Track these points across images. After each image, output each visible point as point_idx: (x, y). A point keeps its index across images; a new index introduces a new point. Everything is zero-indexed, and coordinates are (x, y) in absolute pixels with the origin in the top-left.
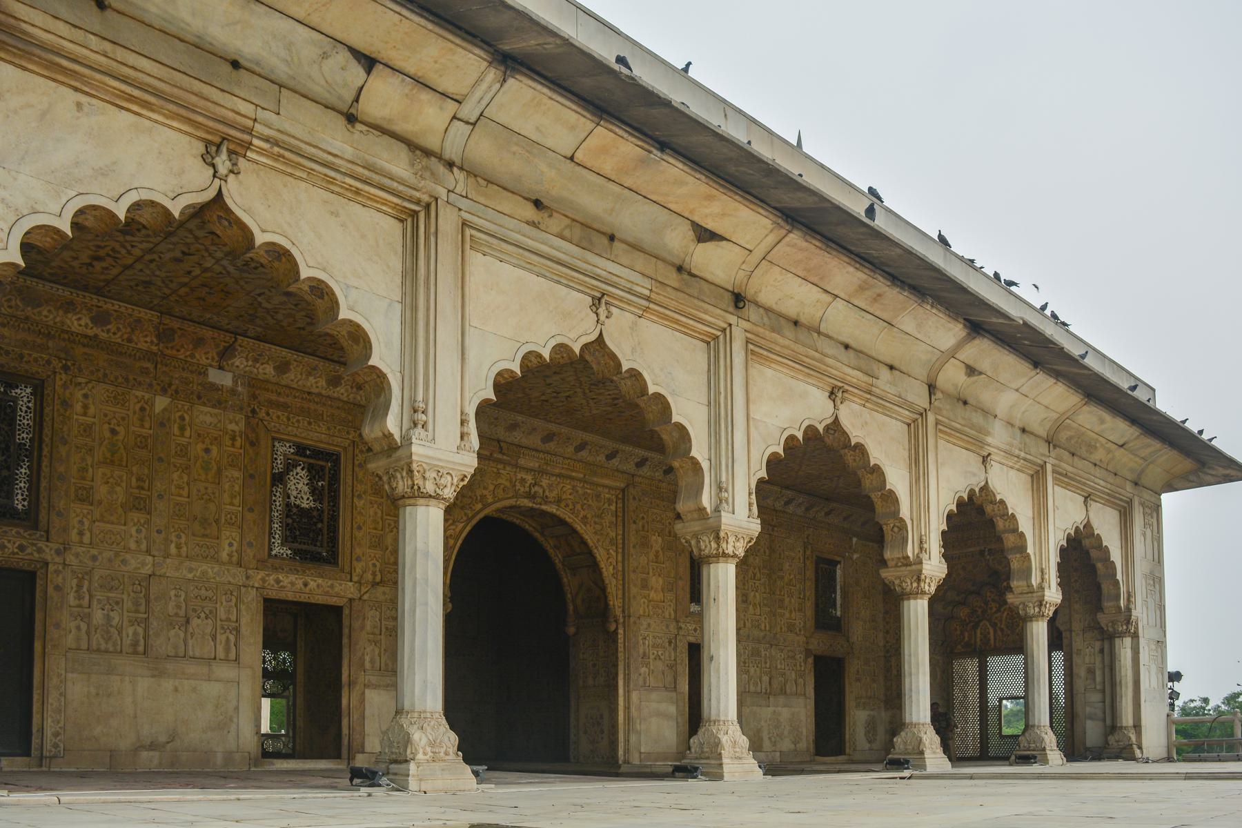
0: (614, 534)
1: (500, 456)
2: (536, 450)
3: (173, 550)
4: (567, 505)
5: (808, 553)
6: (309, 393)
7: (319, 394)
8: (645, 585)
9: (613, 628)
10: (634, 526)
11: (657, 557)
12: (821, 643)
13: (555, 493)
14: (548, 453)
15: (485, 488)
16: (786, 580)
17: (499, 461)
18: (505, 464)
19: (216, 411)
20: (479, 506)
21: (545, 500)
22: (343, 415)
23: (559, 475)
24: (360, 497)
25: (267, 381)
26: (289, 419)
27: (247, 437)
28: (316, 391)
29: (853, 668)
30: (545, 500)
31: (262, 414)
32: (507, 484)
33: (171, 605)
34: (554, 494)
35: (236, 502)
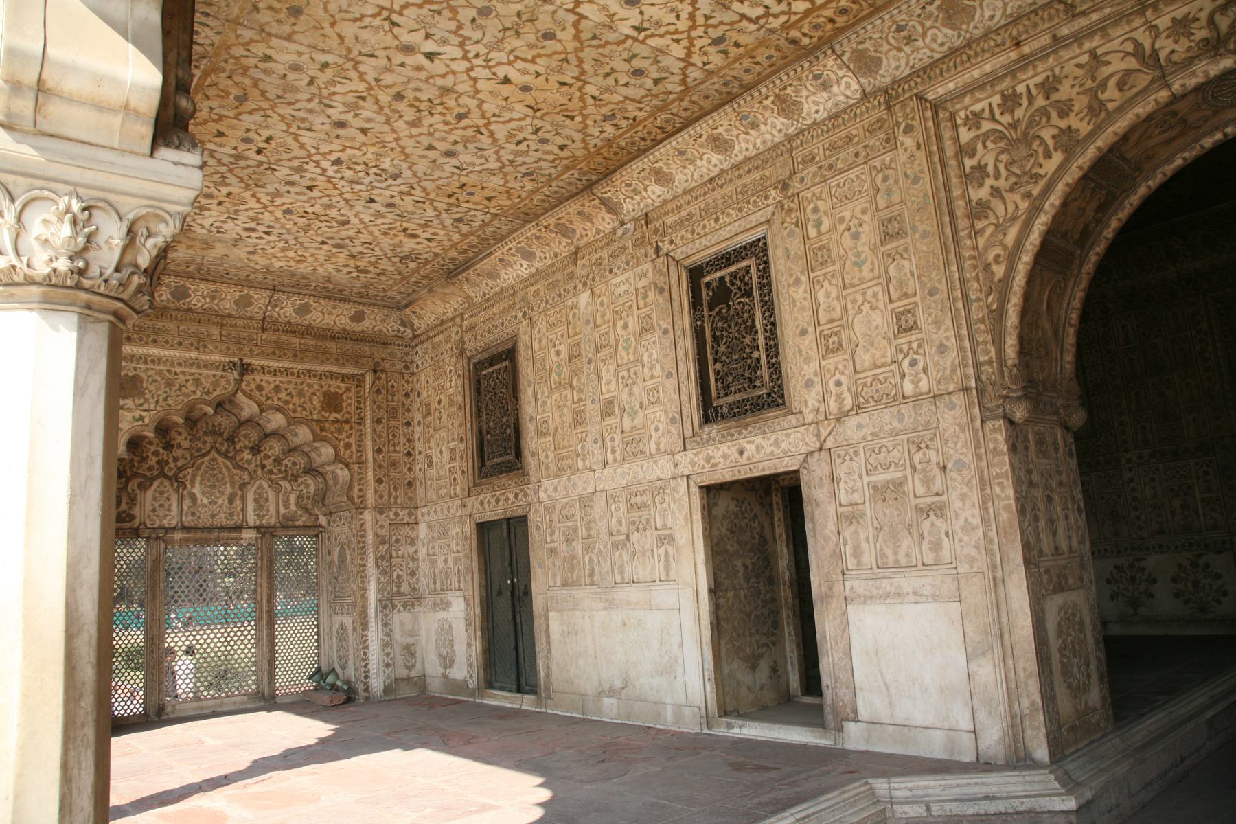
1: (1083, 22)
3: (610, 457)
6: (711, 180)
7: (722, 171)
15: (1063, 114)
17: (1078, 38)
18: (1101, 29)
19: (622, 278)
20: (1058, 157)
22: (757, 175)
24: (797, 282)
25: (665, 202)
26: (693, 232)
27: (656, 285)
28: (716, 171)
31: (665, 247)
32: (1132, 63)
33: (614, 520)
35: (656, 372)
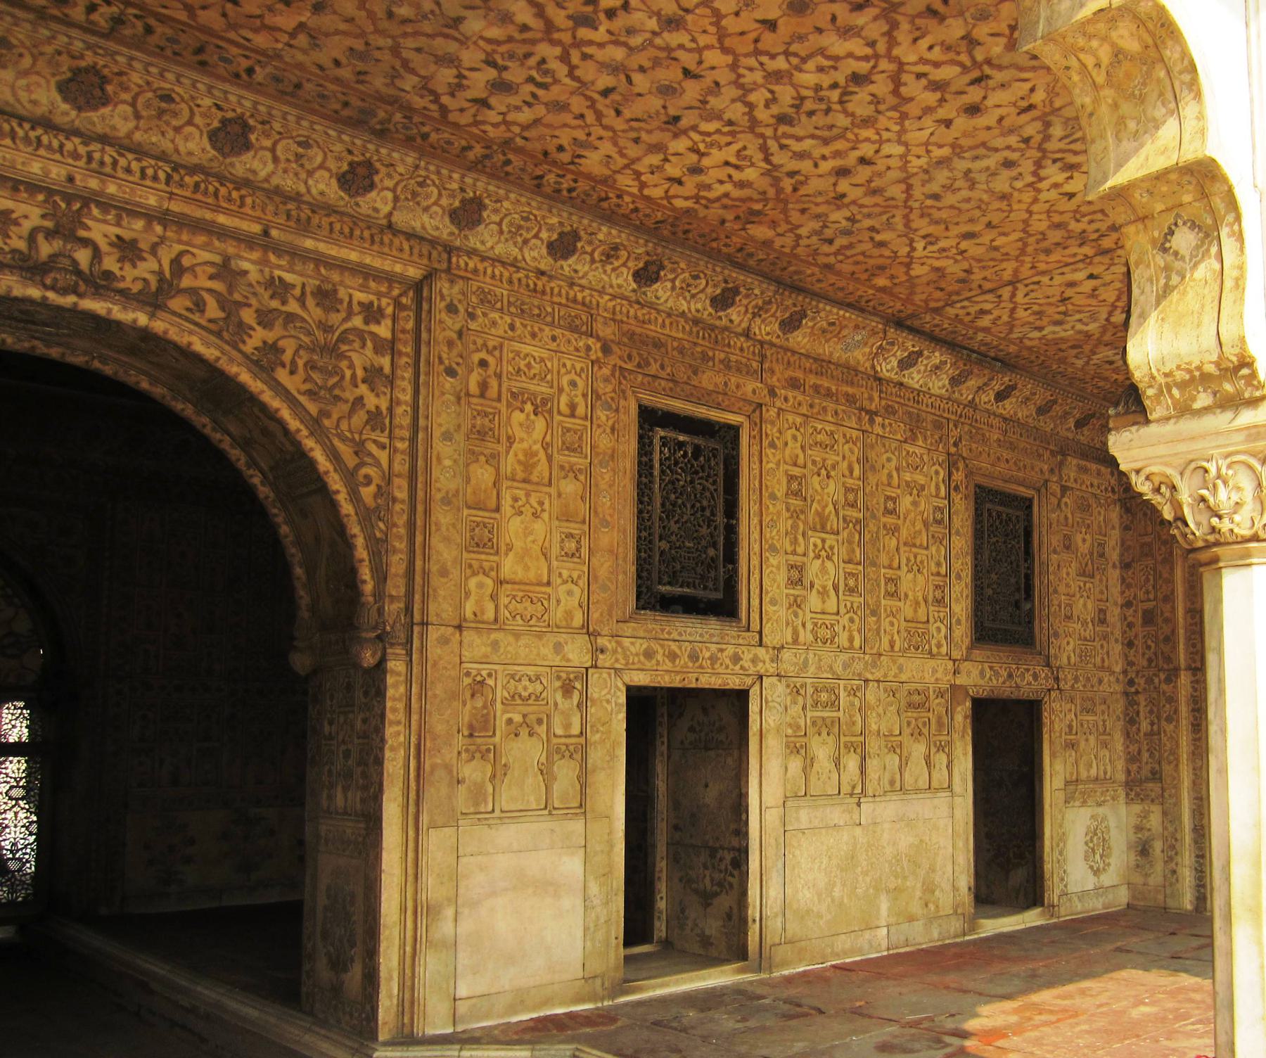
0: (384, 406)
2: (47, 124)
4: (200, 306)
5: (958, 476)
8: (484, 542)
9: (368, 658)
10: (449, 382)
11: (528, 466)
12: (984, 674)
13: (146, 268)
14: (104, 139)
16: (904, 533)
21: (102, 283)
23: (164, 218)
29: (1058, 720)
30: (102, 283)
34: (146, 268)
